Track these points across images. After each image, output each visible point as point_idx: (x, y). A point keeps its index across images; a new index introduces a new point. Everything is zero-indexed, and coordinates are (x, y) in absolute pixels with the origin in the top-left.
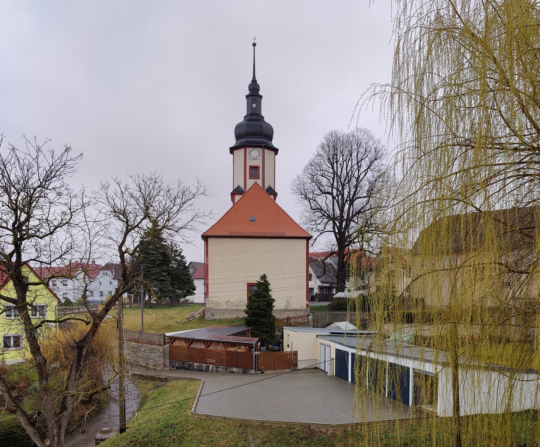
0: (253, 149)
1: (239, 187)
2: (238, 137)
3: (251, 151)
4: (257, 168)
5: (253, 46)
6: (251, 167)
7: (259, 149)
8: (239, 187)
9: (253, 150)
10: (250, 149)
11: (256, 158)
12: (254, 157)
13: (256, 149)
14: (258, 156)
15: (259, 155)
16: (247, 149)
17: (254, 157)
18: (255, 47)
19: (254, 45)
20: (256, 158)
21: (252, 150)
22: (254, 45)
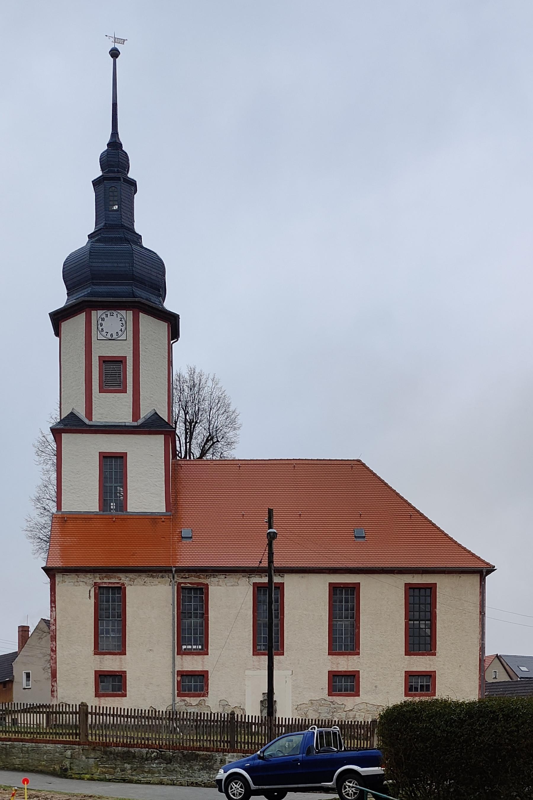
0: (108, 313)
1: (72, 416)
2: (71, 288)
3: (103, 319)
4: (120, 361)
5: (112, 57)
6: (104, 362)
7: (123, 312)
8: (72, 416)
9: (107, 315)
10: (100, 312)
11: (115, 336)
12: (112, 335)
13: (115, 313)
14: (120, 333)
15: (123, 328)
16: (94, 313)
17: (112, 335)
18: (117, 59)
19: (115, 54)
20: (115, 336)
21: (104, 316)
22: (115, 54)
